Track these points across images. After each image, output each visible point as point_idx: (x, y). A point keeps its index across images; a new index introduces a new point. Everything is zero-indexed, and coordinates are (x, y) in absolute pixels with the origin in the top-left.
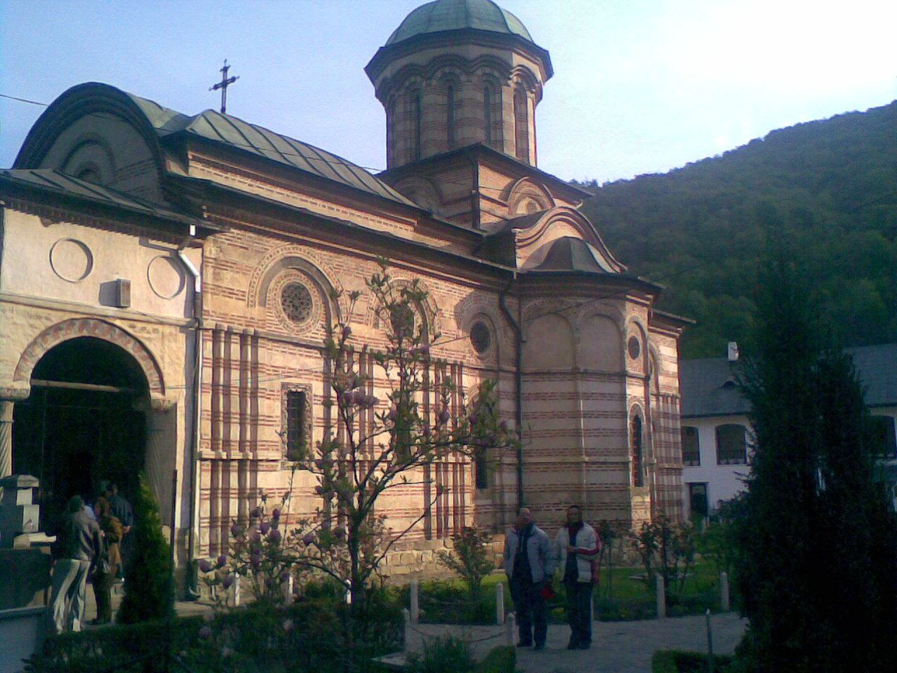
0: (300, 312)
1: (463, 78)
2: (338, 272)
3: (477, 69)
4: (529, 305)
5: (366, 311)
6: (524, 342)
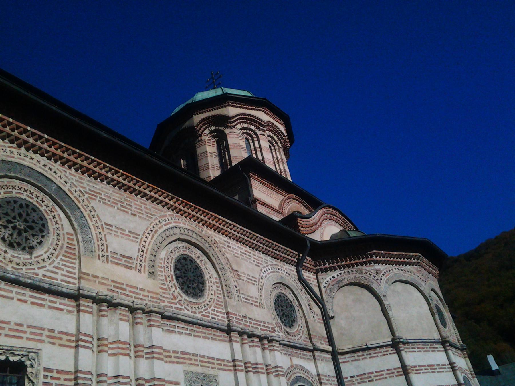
0: (27, 239)
1: (227, 131)
2: (91, 198)
3: (237, 124)
4: (328, 279)
5: (137, 254)
6: (332, 318)
